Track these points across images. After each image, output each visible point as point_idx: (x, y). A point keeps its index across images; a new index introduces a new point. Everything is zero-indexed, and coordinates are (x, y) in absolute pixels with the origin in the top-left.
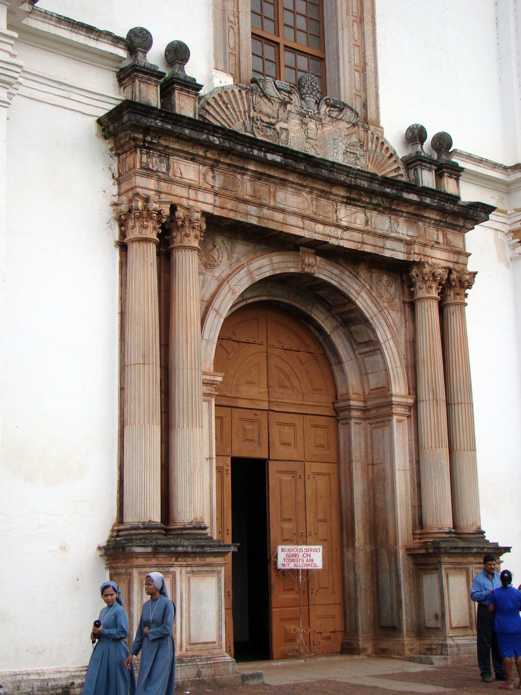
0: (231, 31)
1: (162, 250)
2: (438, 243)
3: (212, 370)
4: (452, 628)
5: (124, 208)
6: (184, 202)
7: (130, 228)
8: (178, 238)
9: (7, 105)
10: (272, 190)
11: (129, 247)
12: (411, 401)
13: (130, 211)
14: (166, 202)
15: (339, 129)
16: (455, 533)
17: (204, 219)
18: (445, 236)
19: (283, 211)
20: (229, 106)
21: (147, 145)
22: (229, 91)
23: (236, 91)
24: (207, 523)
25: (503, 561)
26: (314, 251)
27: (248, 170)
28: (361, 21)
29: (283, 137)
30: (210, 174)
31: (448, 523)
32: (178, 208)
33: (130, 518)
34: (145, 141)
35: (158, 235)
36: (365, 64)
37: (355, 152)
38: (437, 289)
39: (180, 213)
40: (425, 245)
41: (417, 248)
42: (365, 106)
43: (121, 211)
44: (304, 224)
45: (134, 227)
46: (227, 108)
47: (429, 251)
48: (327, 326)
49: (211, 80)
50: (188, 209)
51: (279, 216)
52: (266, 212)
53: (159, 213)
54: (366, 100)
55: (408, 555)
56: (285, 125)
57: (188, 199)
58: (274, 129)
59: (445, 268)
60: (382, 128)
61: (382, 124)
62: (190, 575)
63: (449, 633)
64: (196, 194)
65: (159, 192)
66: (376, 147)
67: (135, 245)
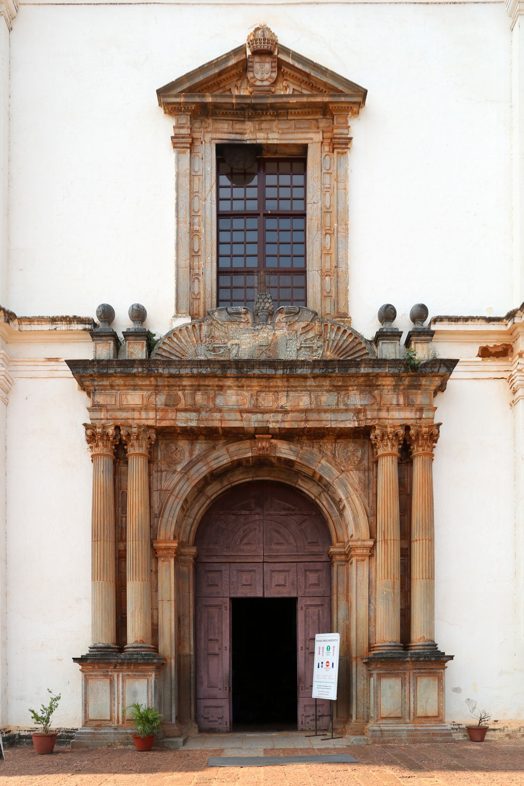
12: (371, 543)
15: (295, 330)
18: (406, 397)
21: (97, 388)
23: (190, 327)
25: (447, 667)
27: (185, 386)
29: (234, 352)
30: (153, 397)
34: (93, 386)
37: (310, 345)
41: (369, 415)
44: (242, 417)
47: (383, 414)
51: (217, 415)
56: (236, 341)
57: (134, 419)
60: (350, 318)
61: (351, 314)
64: (140, 414)
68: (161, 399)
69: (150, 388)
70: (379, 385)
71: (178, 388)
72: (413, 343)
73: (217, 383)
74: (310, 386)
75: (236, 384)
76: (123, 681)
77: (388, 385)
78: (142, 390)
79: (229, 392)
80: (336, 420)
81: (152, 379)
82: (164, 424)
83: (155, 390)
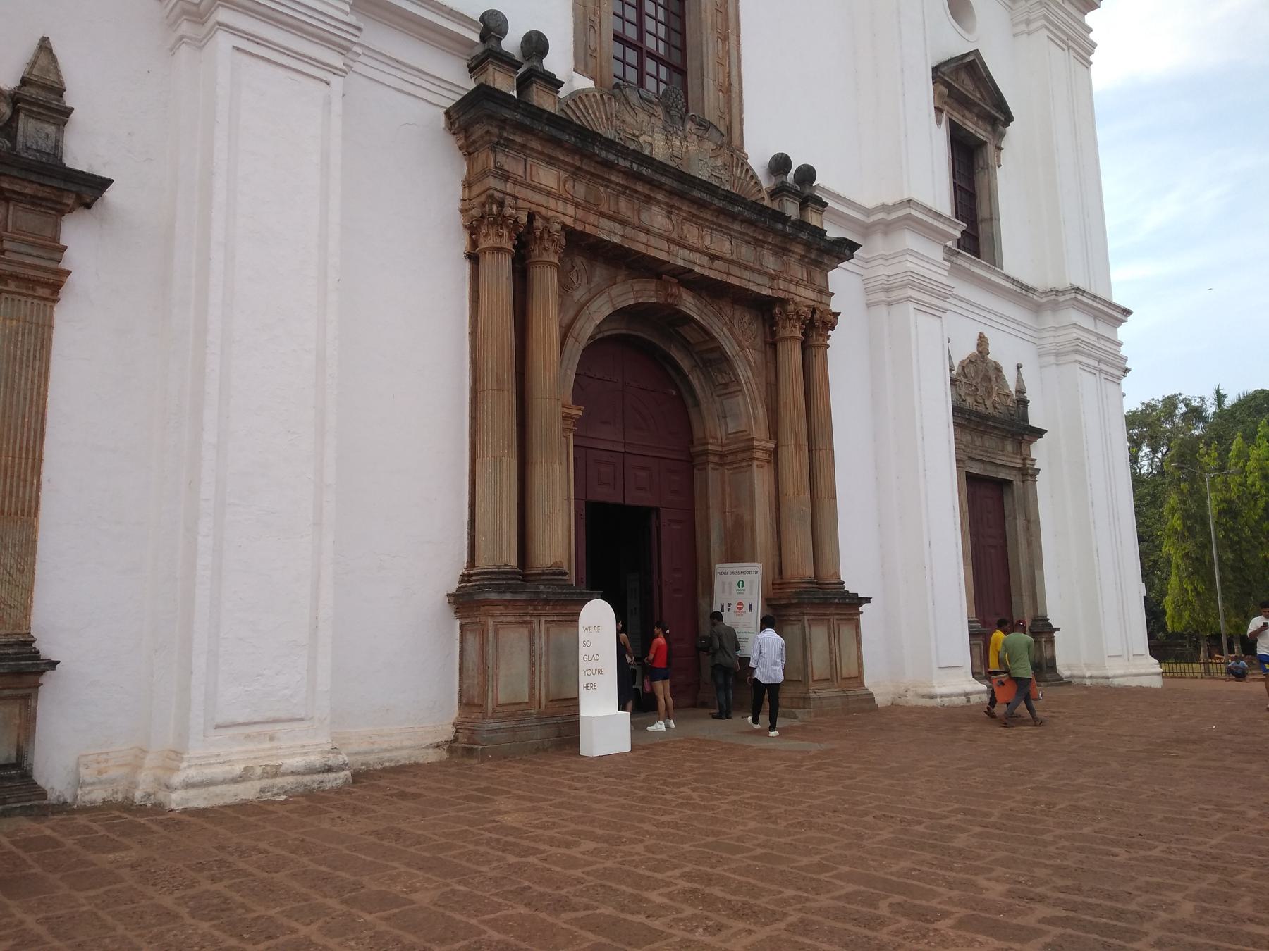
0: (592, 30)
1: (517, 266)
2: (802, 280)
3: (570, 402)
4: (814, 681)
5: (476, 212)
6: (543, 211)
7: (482, 235)
8: (535, 249)
9: (344, 75)
10: (636, 207)
11: (482, 257)
13: (482, 217)
14: (523, 209)
16: (817, 583)
17: (563, 234)
18: (809, 274)
19: (648, 232)
20: (591, 112)
21: (502, 142)
22: (591, 94)
23: (598, 97)
24: (565, 569)
26: (676, 281)
28: (725, 38)
31: (809, 572)
32: (537, 217)
33: (483, 563)
34: (500, 137)
35: (514, 246)
36: (730, 84)
37: (720, 176)
38: (801, 328)
39: (538, 223)
40: (790, 281)
42: (729, 129)
43: (473, 217)
45: (487, 235)
46: (588, 113)
48: (685, 364)
49: (571, 81)
50: (547, 219)
51: (642, 237)
52: (629, 231)
53: (516, 221)
54: (731, 123)
55: (768, 605)
56: (649, 139)
57: (548, 208)
58: (638, 142)
59: (808, 306)
61: (747, 149)
62: (549, 625)
63: (813, 686)
65: (516, 198)
66: (741, 173)
67: (489, 257)
68: (580, 190)
69: (569, 168)
70: (790, 251)
71: (602, 182)
72: (810, 209)
73: (647, 192)
74: (736, 231)
75: (667, 200)
76: (547, 630)
77: (797, 254)
78: (559, 167)
79: (655, 209)
80: (754, 282)
81: (577, 157)
82: (579, 227)
83: (574, 173)
